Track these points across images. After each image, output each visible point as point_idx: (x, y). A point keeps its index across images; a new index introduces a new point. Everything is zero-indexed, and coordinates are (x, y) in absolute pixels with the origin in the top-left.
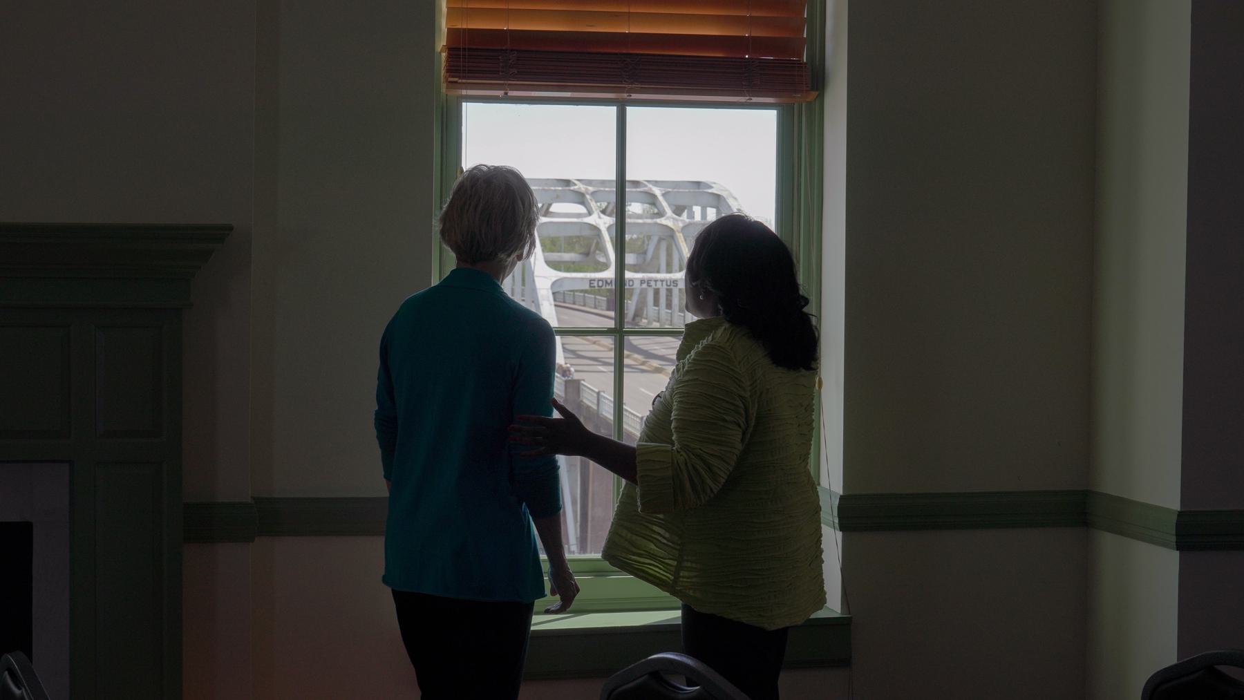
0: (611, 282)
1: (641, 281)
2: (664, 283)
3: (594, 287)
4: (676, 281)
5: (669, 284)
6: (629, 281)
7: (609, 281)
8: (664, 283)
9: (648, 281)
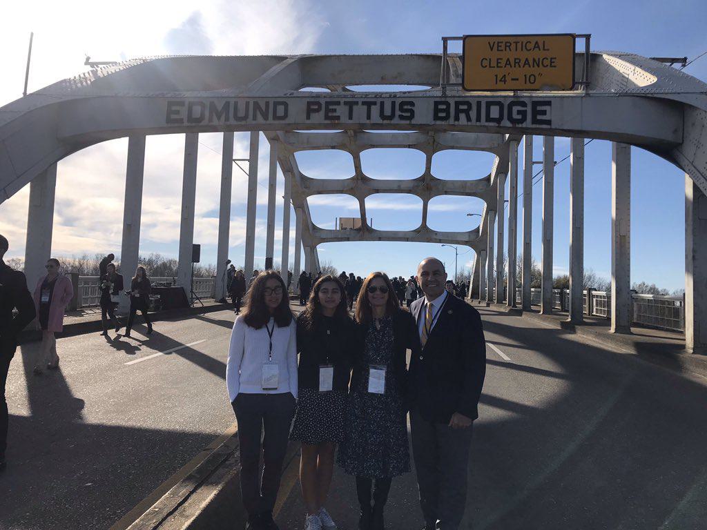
0: (227, 104)
1: (309, 104)
2: (375, 110)
3: (181, 121)
4: (412, 104)
5: (388, 112)
6: (276, 104)
7: (220, 106)
8: (375, 110)
9: (328, 103)
